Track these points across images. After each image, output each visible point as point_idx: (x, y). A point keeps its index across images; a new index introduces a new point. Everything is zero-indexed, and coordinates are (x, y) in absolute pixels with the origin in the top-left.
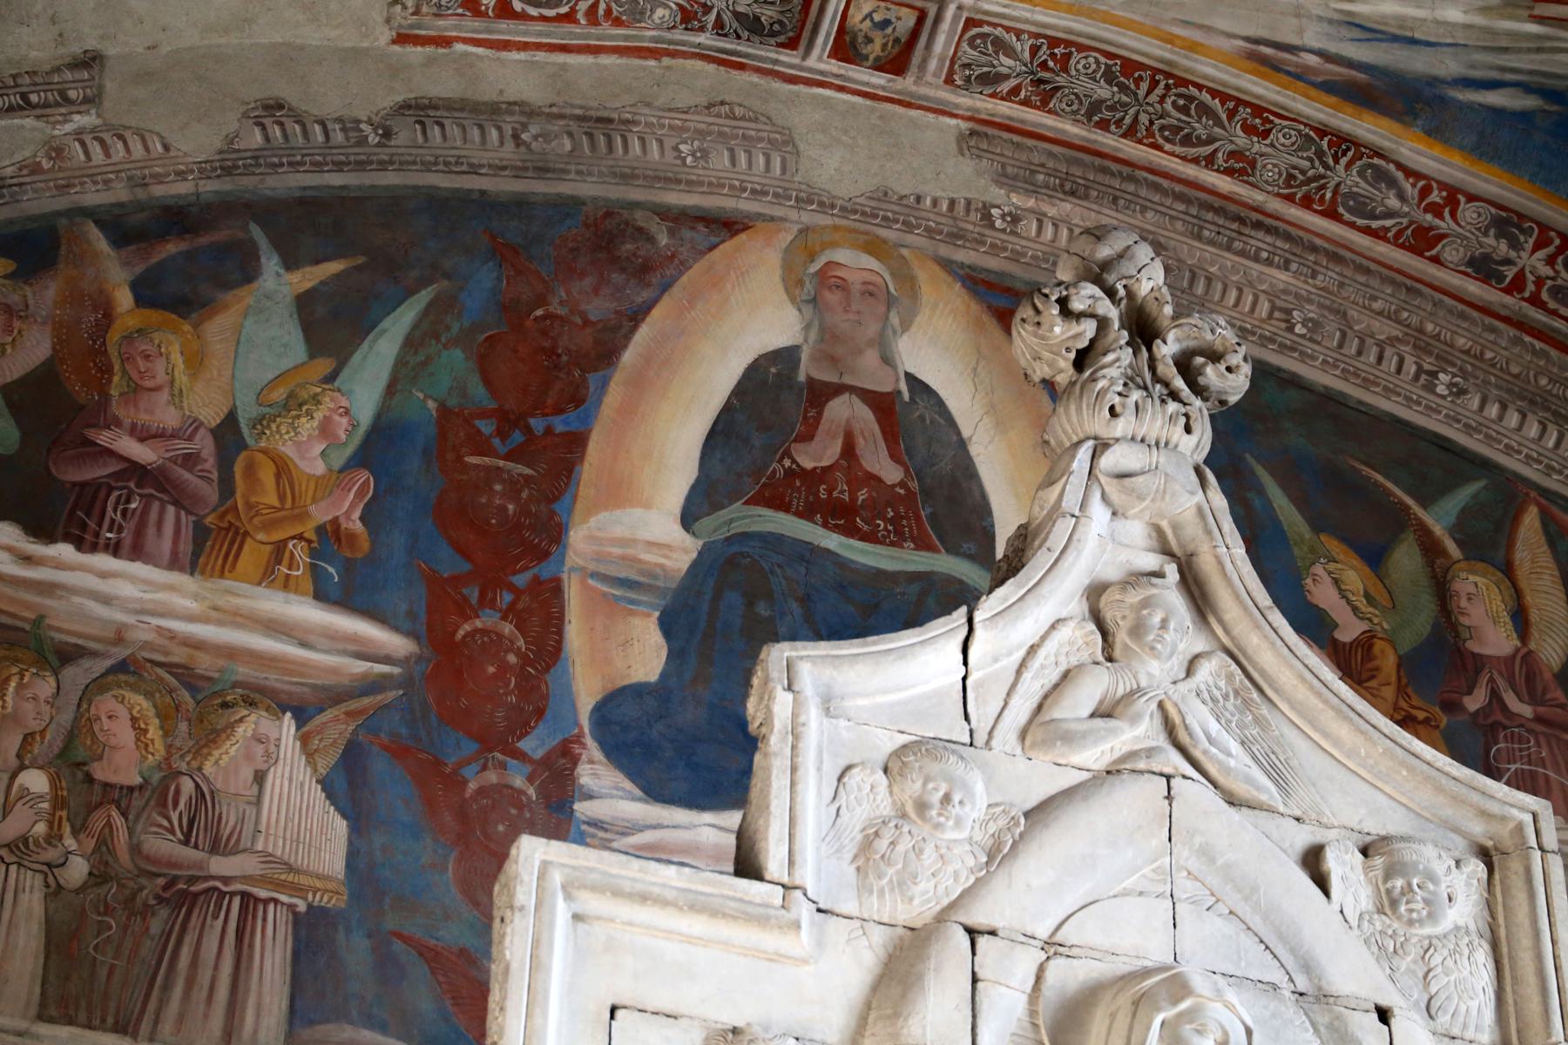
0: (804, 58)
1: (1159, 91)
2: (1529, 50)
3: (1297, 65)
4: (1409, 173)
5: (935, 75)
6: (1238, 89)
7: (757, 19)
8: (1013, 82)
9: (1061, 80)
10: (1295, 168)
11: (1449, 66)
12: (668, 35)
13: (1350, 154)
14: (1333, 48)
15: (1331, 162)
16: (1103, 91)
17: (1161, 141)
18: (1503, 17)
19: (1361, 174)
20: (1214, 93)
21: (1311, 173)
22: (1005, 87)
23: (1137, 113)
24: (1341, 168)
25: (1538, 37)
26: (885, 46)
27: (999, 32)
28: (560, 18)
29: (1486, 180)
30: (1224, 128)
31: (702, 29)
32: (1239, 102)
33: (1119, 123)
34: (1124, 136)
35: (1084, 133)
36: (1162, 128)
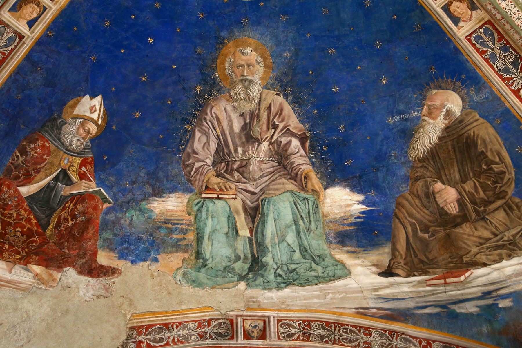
0: (237, 341)
1: (338, 329)
2: (430, 295)
3: (371, 313)
4: (414, 338)
5: (275, 338)
6: (358, 323)
7: (220, 333)
8: (297, 335)
9: (310, 332)
10: (382, 343)
11: (411, 304)
12: (198, 343)
13: (395, 335)
14: (378, 306)
15: (391, 339)
16: (323, 332)
17: (343, 343)
18: (420, 287)
19: (401, 341)
20: (352, 326)
21: (387, 343)
22: (295, 337)
23: (334, 336)
24: (394, 340)
25: (431, 291)
26: (258, 332)
27: (287, 321)
28: (165, 345)
29: (436, 335)
30: (359, 335)
31: (207, 339)
32: (360, 327)
33: (330, 340)
34: (333, 344)
35: (322, 346)
36: (342, 339)
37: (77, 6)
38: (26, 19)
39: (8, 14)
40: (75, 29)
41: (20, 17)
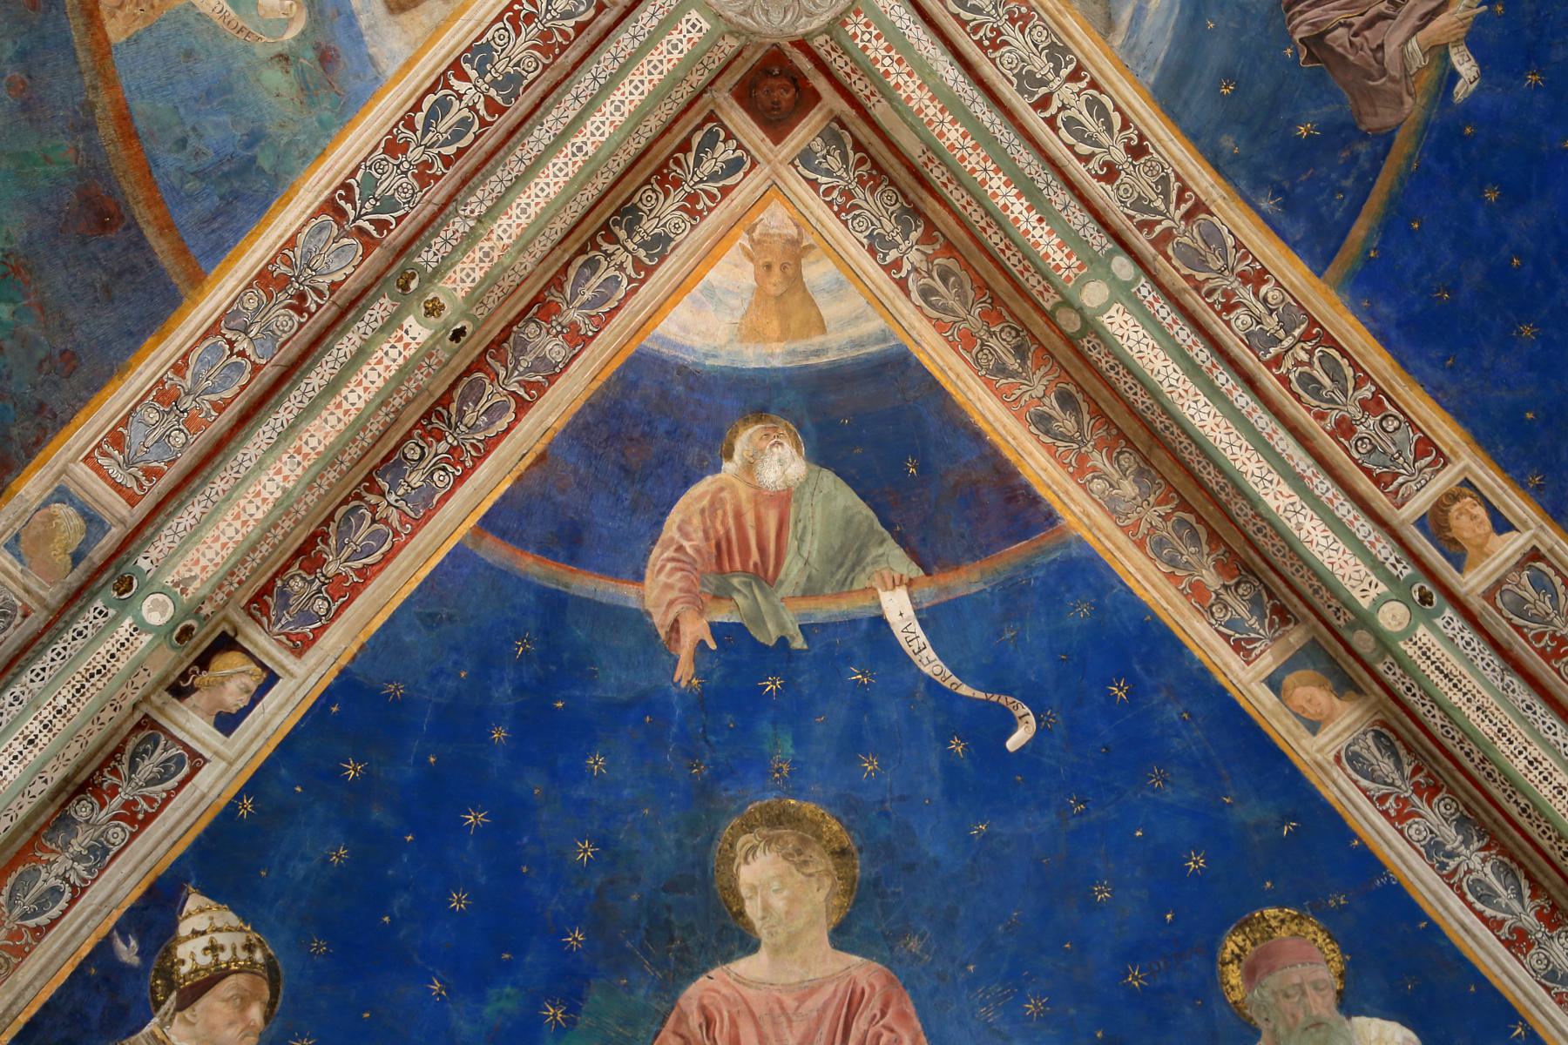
37: (1468, 402)
38: (1487, 536)
39: (1468, 576)
40: (1529, 416)
41: (1480, 547)
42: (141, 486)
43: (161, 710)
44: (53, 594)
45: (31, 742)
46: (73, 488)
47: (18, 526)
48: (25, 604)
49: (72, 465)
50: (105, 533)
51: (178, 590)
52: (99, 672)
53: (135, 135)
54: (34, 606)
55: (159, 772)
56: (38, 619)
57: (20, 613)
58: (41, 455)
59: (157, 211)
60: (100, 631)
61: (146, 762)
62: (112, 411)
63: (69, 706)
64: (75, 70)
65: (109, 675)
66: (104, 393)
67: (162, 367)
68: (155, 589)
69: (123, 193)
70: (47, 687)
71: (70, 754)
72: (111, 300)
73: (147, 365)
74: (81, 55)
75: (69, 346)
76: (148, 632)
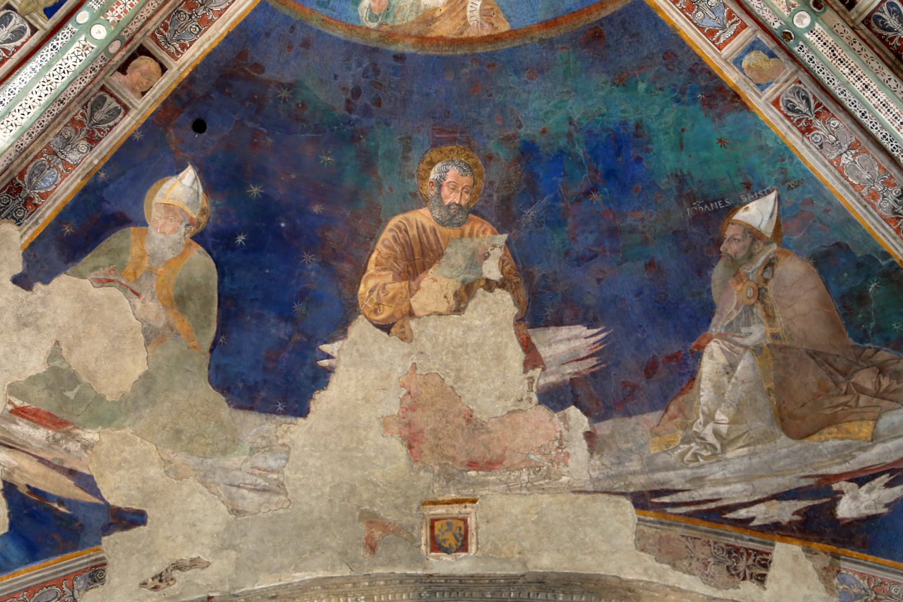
42: (736, 22)
43: (860, 14)
44: (790, 68)
45: (866, 87)
46: (735, 56)
47: (752, 84)
48: (794, 82)
49: (723, 56)
50: (760, 40)
51: (792, 9)
52: (833, 51)
53: (555, 19)
54: (795, 77)
55: (895, 16)
56: (802, 76)
57: (798, 85)
58: (716, 71)
59: (594, 9)
60: (810, 50)
61: (889, 22)
62: (695, 35)
63: (849, 67)
64: (523, 47)
65: (835, 46)
66: (686, 39)
67: (674, 10)
68: (790, 21)
69: (584, 26)
70: (837, 77)
71: (876, 66)
72: (638, 34)
73: (673, 16)
74: (516, 44)
75: (661, 55)
76: (814, 25)
